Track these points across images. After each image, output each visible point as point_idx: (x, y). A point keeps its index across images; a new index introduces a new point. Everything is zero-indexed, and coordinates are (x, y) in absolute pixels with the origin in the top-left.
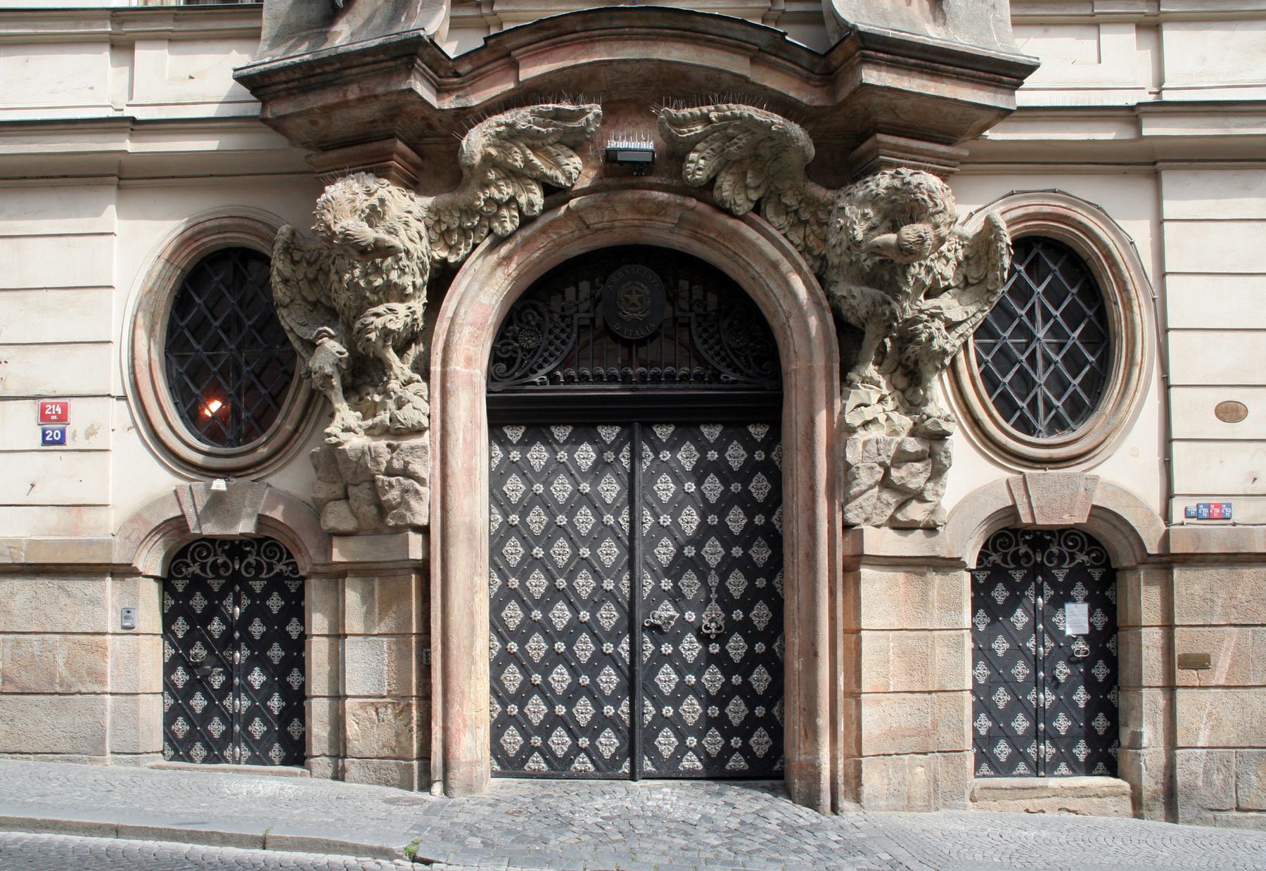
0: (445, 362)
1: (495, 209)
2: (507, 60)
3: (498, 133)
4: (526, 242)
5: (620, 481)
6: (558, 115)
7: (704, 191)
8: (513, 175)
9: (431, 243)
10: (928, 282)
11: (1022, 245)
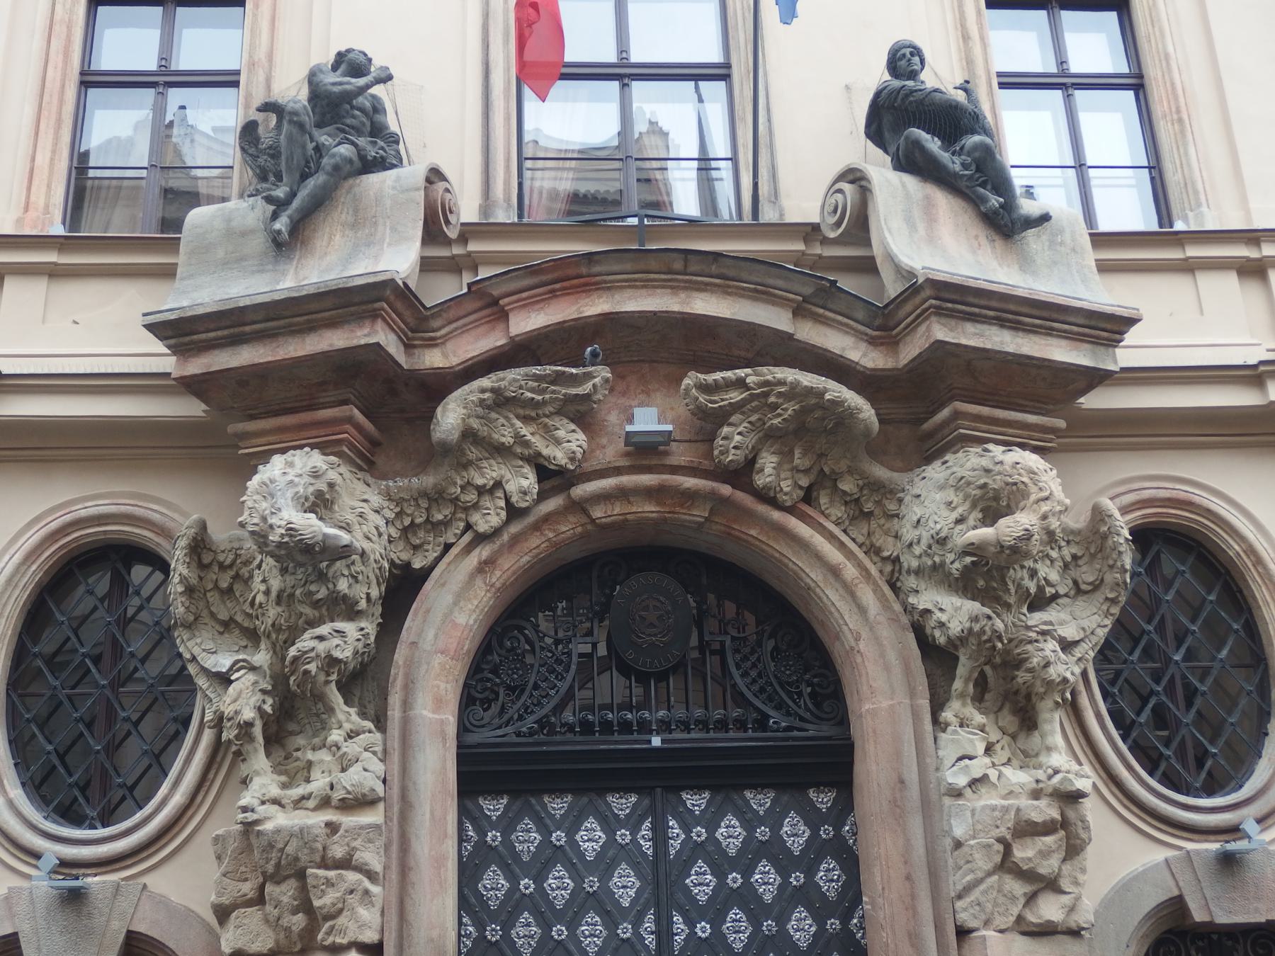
0: (406, 705)
1: (471, 497)
2: (495, 309)
3: (482, 401)
4: (515, 540)
5: (639, 875)
6: (558, 379)
7: (741, 475)
8: (500, 451)
9: (390, 542)
10: (1033, 590)
11: (1143, 536)
